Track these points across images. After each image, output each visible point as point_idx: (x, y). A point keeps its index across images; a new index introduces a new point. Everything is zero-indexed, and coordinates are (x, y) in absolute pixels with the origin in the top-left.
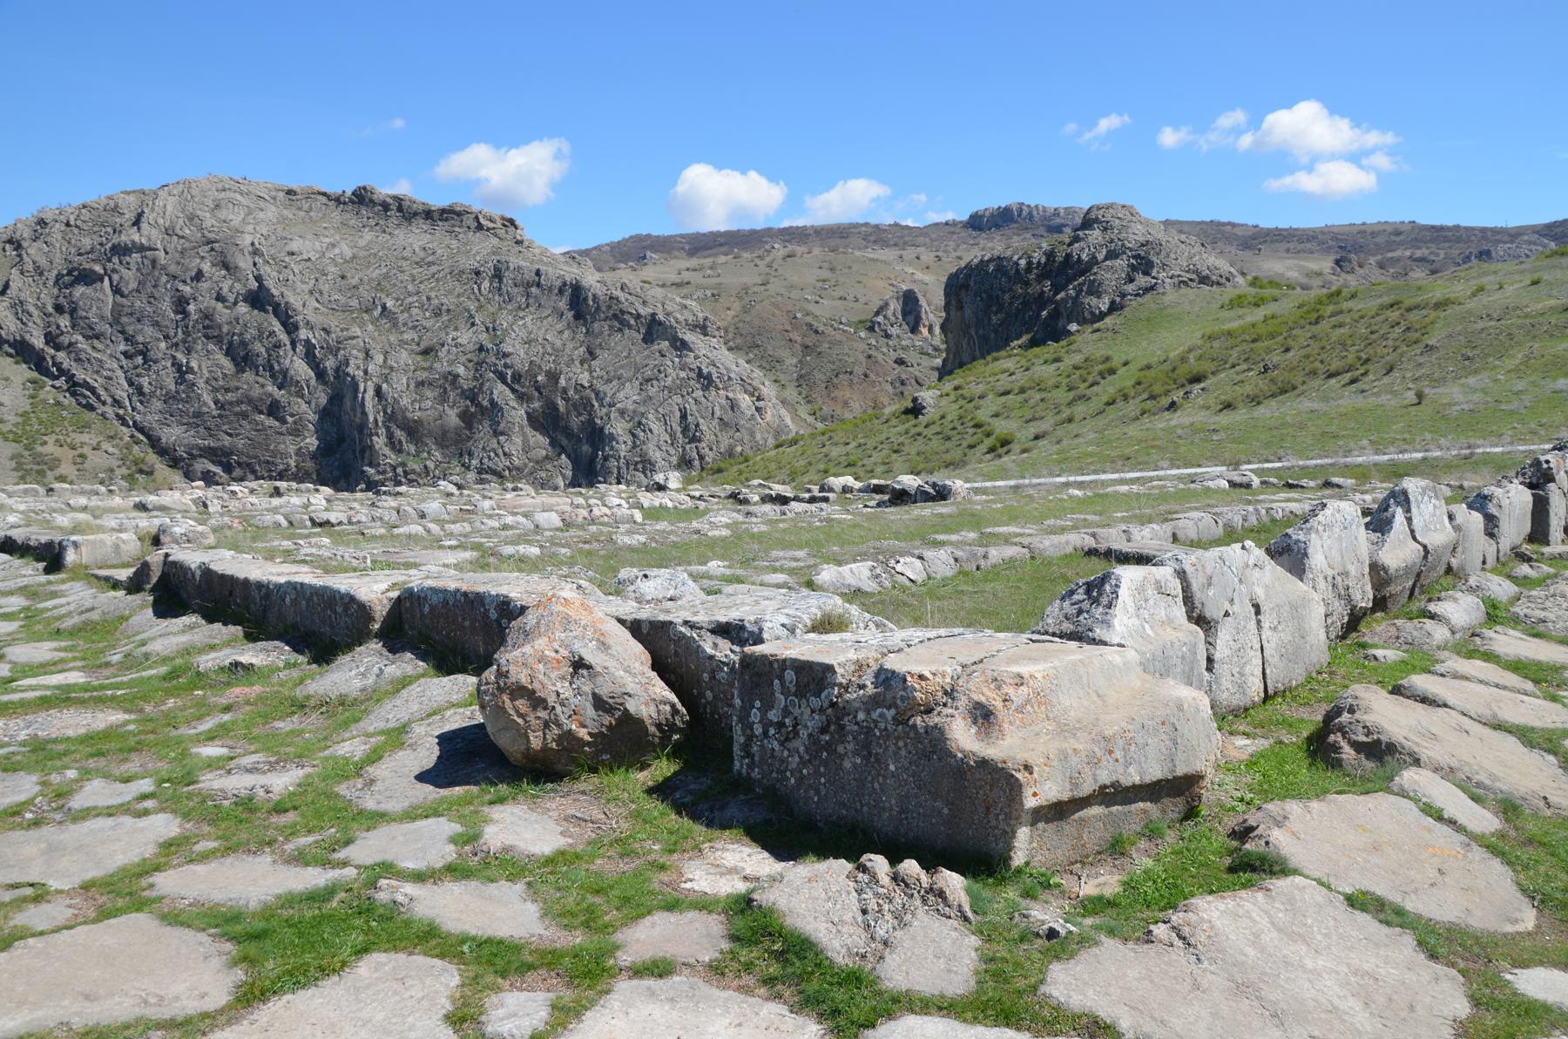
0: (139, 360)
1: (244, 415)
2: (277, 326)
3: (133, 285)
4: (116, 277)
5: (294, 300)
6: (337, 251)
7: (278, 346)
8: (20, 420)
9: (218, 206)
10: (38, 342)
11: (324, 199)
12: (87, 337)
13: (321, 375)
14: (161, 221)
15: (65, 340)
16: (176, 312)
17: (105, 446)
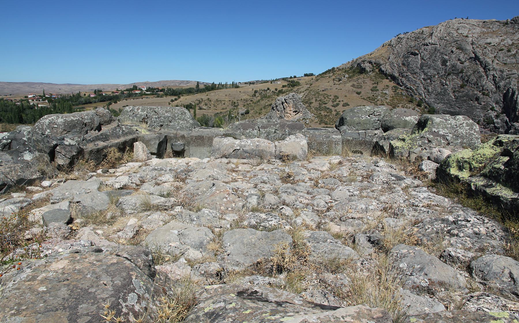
0: (429, 81)
1: (465, 101)
2: (481, 70)
3: (428, 56)
4: (422, 54)
5: (489, 61)
6: (505, 42)
7: (481, 77)
8: (391, 99)
9: (458, 29)
10: (396, 75)
11: (498, 24)
12: (412, 74)
13: (498, 88)
14: (439, 35)
15: (405, 74)
16: (442, 65)
17: (416, 109)
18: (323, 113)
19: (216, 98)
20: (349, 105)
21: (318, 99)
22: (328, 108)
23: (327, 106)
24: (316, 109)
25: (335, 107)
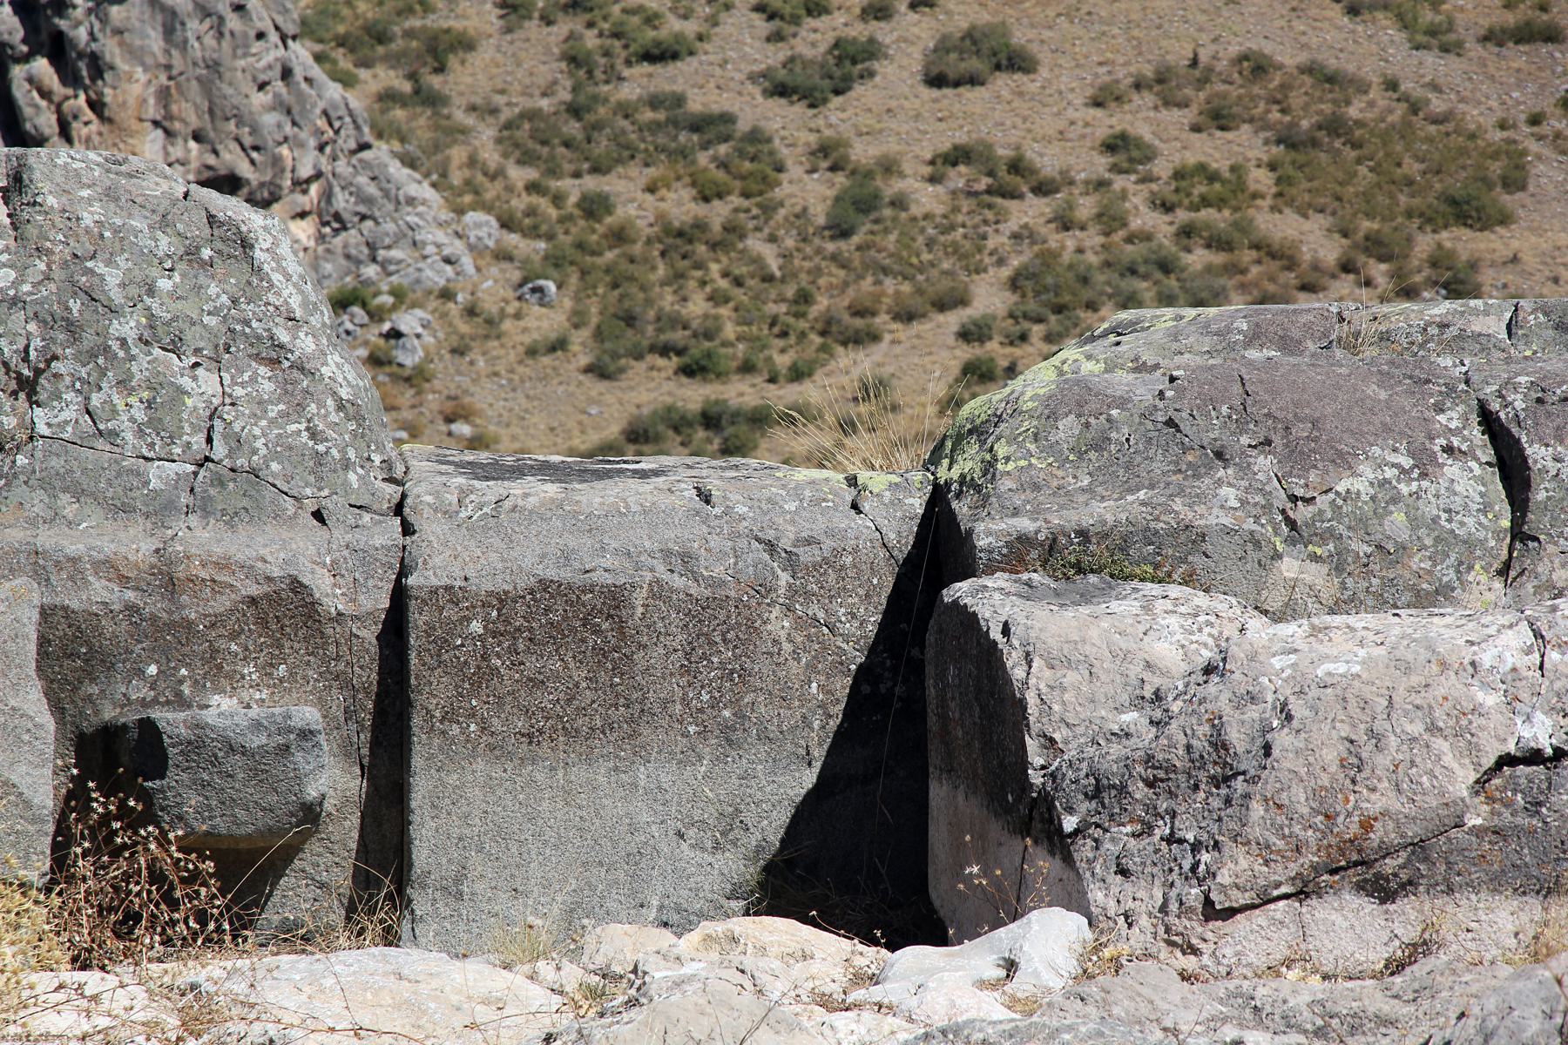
18: (635, 198)
20: (1016, 62)
22: (712, 126)
23: (701, 85)
24: (530, 137)
25: (814, 101)
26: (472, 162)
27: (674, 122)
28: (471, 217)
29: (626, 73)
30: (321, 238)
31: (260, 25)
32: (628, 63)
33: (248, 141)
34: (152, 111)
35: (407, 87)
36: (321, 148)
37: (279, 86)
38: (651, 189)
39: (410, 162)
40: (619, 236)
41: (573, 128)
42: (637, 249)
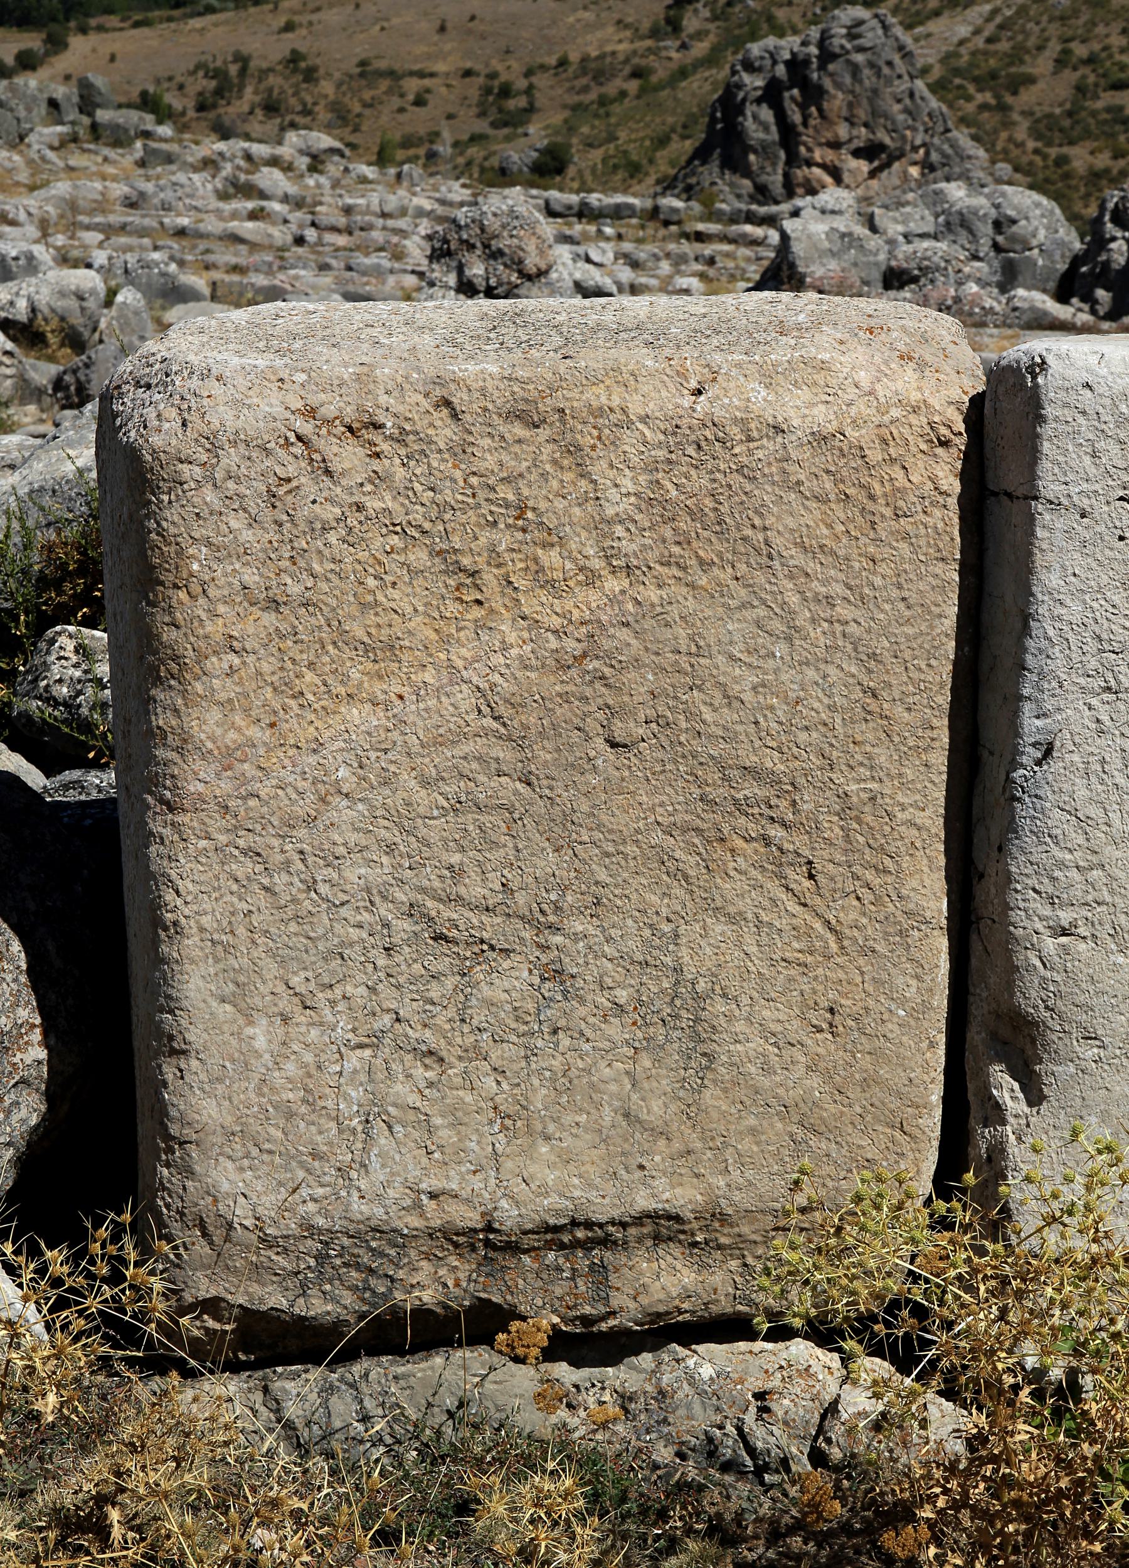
19: (361, 50)
21: (1080, 50)
26: (1010, 139)
27: (1115, 121)
28: (1000, 165)
29: (1102, 95)
30: (923, 174)
31: (899, 71)
32: (1105, 90)
33: (890, 127)
34: (845, 113)
35: (993, 102)
36: (926, 131)
37: (907, 101)
38: (1092, 153)
39: (975, 138)
40: (1067, 176)
41: (1066, 123)
42: (1074, 182)
